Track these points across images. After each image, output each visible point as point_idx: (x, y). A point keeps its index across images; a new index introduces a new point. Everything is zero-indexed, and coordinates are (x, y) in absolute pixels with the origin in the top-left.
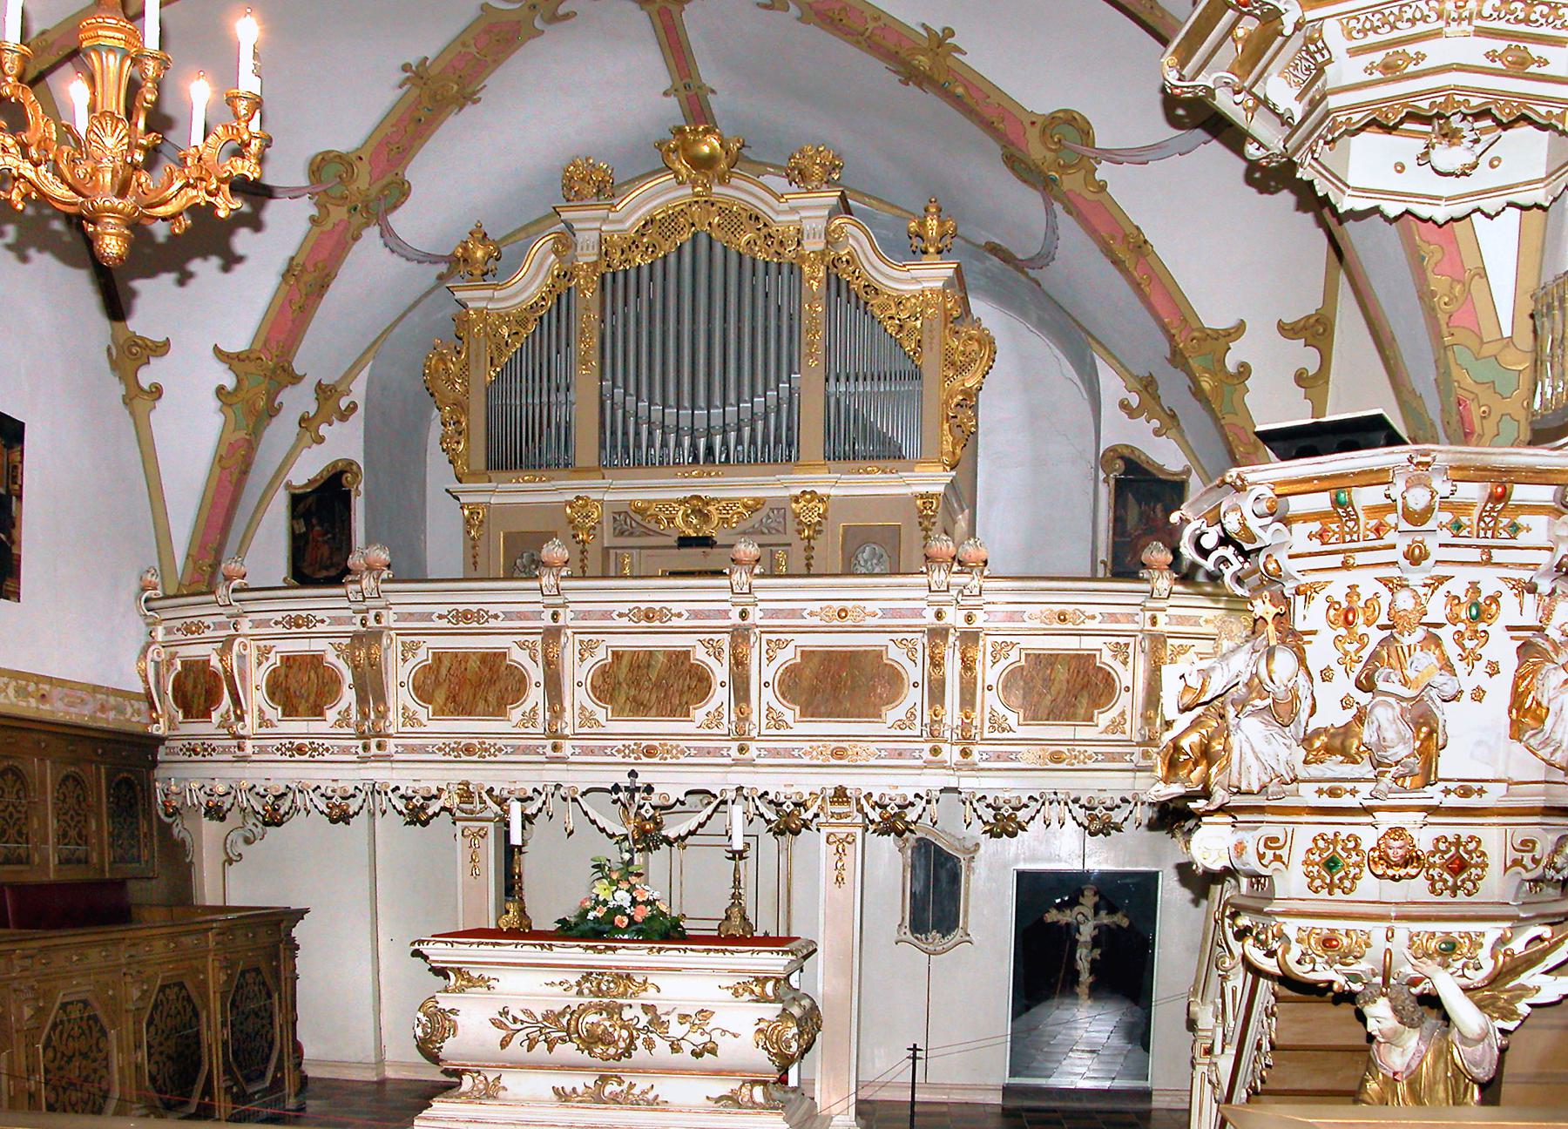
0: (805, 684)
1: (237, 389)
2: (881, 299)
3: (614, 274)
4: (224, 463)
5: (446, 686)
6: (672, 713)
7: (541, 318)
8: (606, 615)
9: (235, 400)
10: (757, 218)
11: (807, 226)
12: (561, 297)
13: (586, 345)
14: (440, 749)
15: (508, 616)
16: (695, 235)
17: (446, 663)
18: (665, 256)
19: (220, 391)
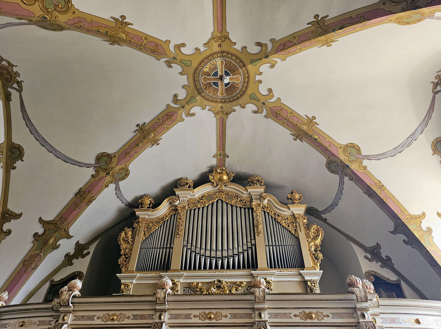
1: (42, 234)
2: (280, 218)
3: (191, 210)
4: (25, 263)
9: (41, 238)
10: (237, 196)
16: (218, 201)
18: (208, 206)
19: (36, 235)
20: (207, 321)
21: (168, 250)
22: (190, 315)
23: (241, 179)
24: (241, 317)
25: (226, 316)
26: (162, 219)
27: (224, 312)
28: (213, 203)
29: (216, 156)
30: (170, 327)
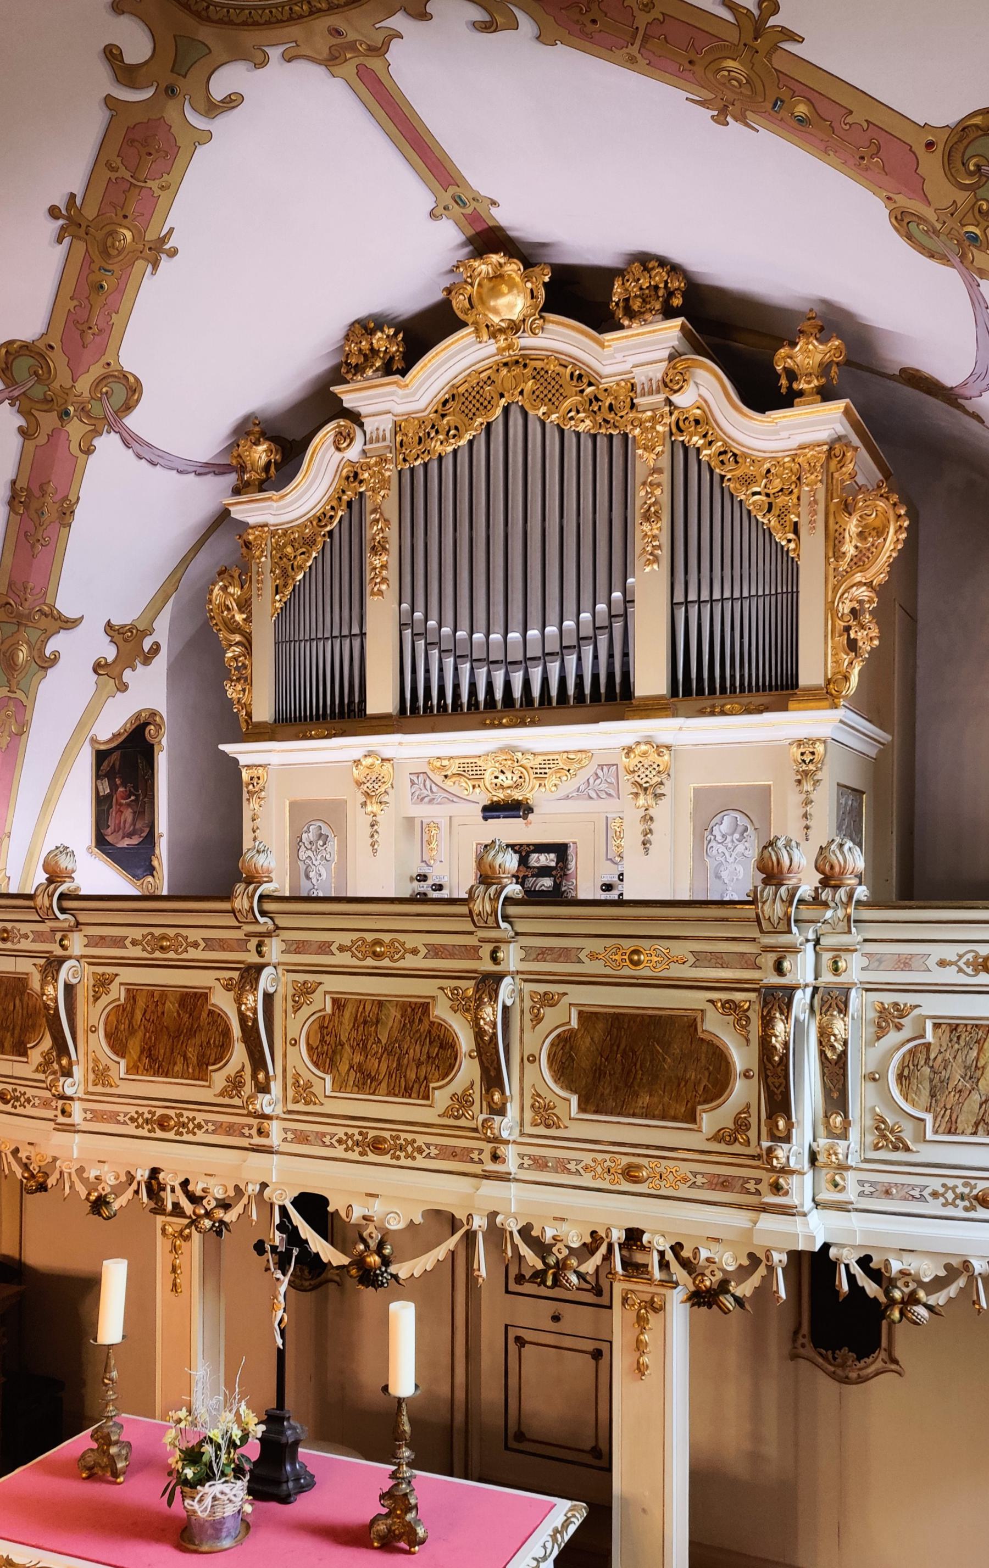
0: (585, 1064)
5: (140, 1034)
6: (408, 1092)
7: (330, 533)
8: (324, 948)
11: (640, 377)
12: (351, 504)
13: (384, 565)
14: (132, 1119)
15: (210, 944)
16: (506, 410)
17: (141, 1003)
18: (471, 442)
20: (370, 962)
21: (357, 643)
22: (330, 944)
23: (581, 294)
24: (452, 956)
25: (415, 952)
26: (322, 519)
27: (411, 941)
28: (489, 425)
29: (440, 210)
30: (288, 971)
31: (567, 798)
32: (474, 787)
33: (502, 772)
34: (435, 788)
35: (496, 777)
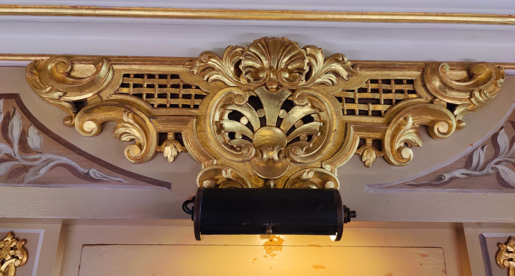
31: (437, 181)
32: (162, 138)
33: (255, 103)
34: (35, 139)
35: (236, 116)
